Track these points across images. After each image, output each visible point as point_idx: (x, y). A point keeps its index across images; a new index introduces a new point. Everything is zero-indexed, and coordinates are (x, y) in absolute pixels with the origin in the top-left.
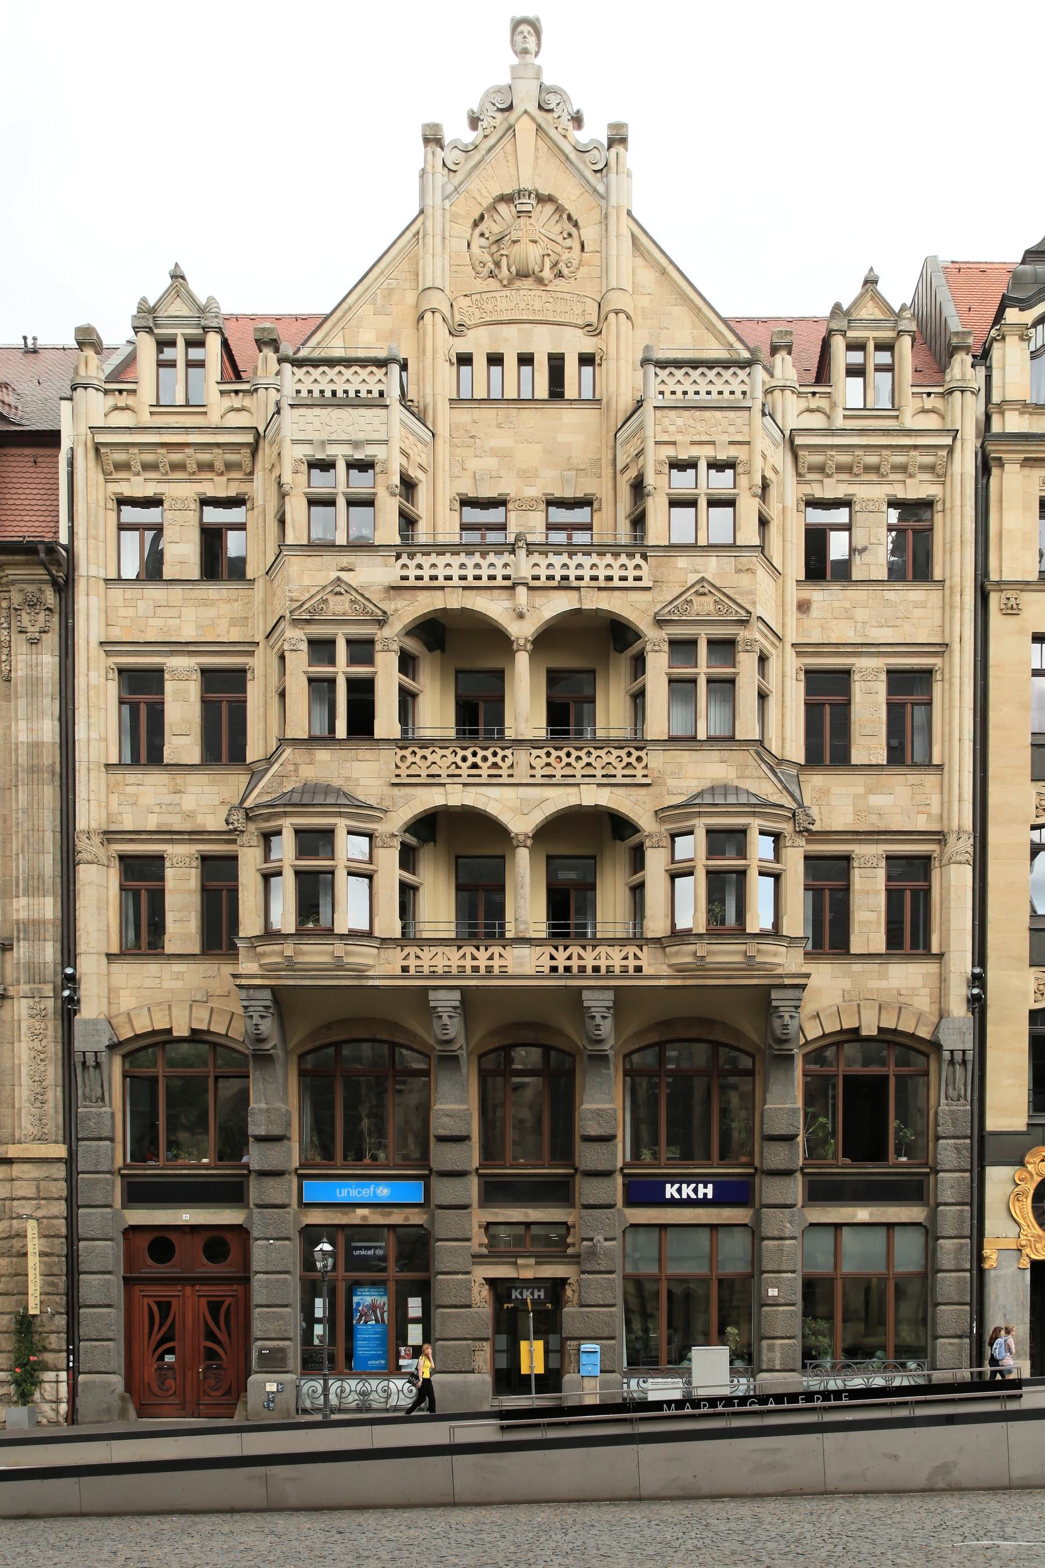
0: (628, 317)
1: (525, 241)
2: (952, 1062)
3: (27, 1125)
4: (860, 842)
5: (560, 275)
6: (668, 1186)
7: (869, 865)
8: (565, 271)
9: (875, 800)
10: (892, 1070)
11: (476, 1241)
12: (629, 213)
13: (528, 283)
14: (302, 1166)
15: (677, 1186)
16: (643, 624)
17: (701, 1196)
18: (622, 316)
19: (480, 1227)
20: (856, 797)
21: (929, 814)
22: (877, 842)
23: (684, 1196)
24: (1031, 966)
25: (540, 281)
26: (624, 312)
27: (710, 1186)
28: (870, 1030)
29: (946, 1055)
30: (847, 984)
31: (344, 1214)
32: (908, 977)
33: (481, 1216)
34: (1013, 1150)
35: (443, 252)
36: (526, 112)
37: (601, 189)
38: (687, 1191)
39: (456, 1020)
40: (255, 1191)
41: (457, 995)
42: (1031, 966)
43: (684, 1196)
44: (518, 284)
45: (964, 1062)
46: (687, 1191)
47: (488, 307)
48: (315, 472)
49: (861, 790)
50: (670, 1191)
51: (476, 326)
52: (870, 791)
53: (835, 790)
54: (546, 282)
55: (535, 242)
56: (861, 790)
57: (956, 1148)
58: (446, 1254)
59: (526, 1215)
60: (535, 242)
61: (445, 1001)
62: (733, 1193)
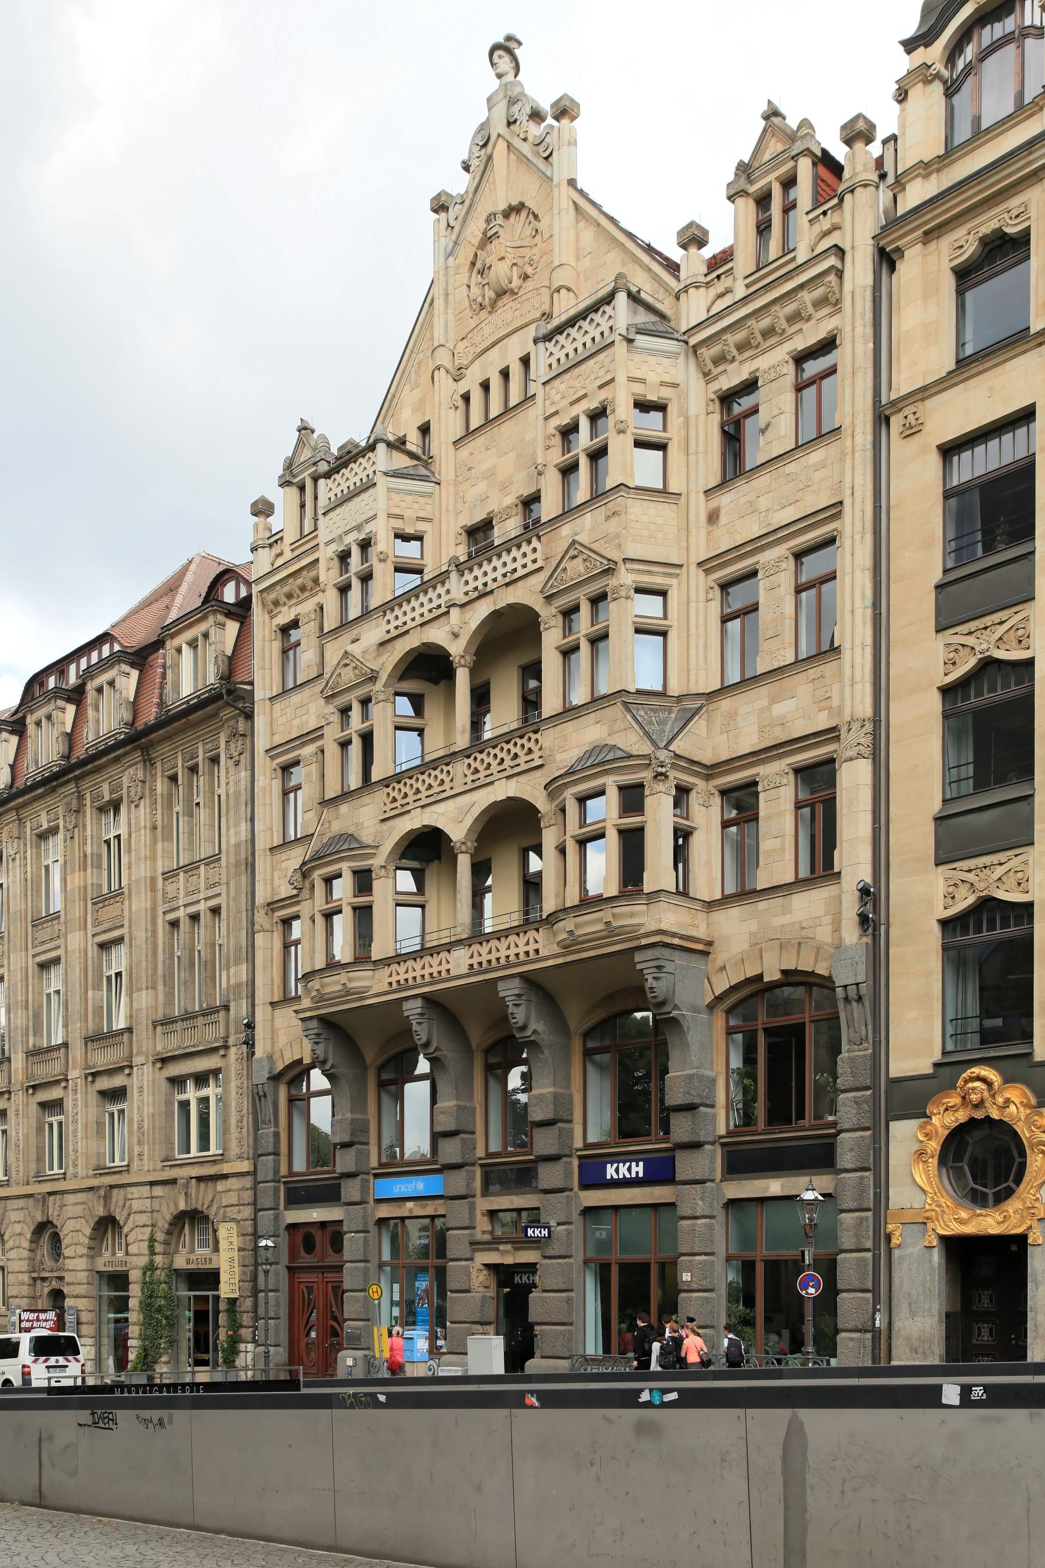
0: (569, 289)
1: (495, 263)
2: (847, 999)
3: (234, 1149)
4: (764, 761)
5: (526, 277)
6: (609, 1166)
7: (772, 785)
8: (529, 271)
9: (778, 709)
10: (807, 1016)
11: (479, 1229)
12: (572, 183)
13: (506, 299)
14: (381, 1165)
15: (628, 1164)
16: (536, 603)
17: (634, 1175)
18: (563, 291)
19: (483, 1215)
20: (761, 711)
21: (830, 708)
22: (779, 757)
23: (621, 1176)
24: (937, 865)
25: (513, 293)
26: (562, 287)
27: (641, 1164)
28: (771, 975)
29: (840, 992)
30: (753, 926)
31: (400, 1207)
32: (809, 906)
33: (484, 1204)
34: (910, 1098)
35: (446, 308)
36: (499, 135)
37: (549, 174)
38: (623, 1170)
39: (522, 1009)
40: (351, 1190)
41: (418, 1003)
42: (937, 865)
43: (621, 1176)
44: (500, 303)
45: (860, 999)
46: (623, 1170)
47: (478, 339)
48: (399, 541)
49: (764, 702)
50: (610, 1171)
51: (472, 362)
52: (773, 701)
53: (742, 710)
54: (516, 291)
55: (503, 258)
56: (764, 702)
57: (856, 1103)
58: (457, 1243)
59: (512, 1202)
60: (503, 258)
61: (413, 1009)
62: (661, 1172)
